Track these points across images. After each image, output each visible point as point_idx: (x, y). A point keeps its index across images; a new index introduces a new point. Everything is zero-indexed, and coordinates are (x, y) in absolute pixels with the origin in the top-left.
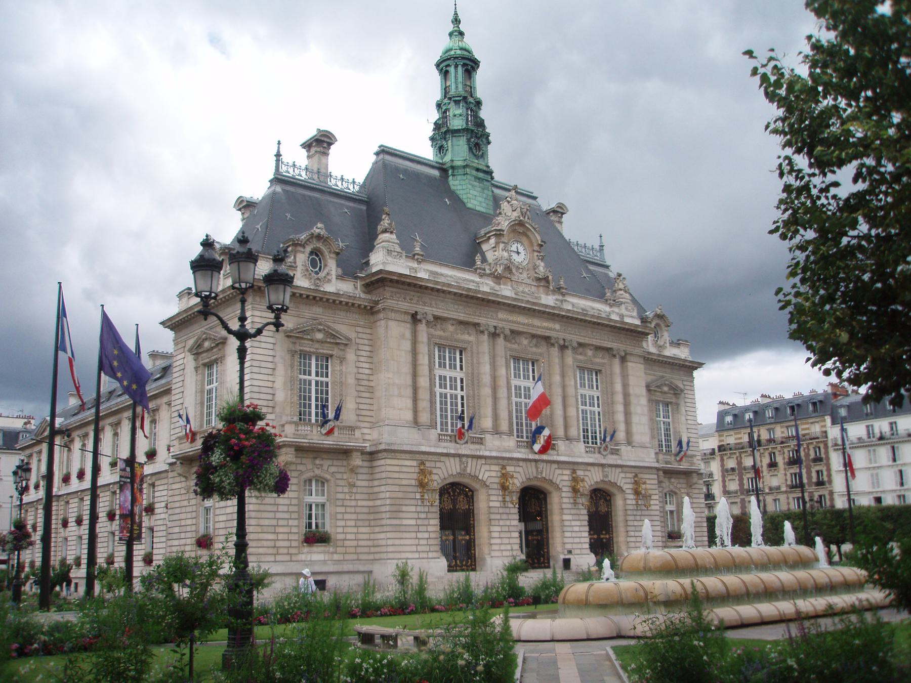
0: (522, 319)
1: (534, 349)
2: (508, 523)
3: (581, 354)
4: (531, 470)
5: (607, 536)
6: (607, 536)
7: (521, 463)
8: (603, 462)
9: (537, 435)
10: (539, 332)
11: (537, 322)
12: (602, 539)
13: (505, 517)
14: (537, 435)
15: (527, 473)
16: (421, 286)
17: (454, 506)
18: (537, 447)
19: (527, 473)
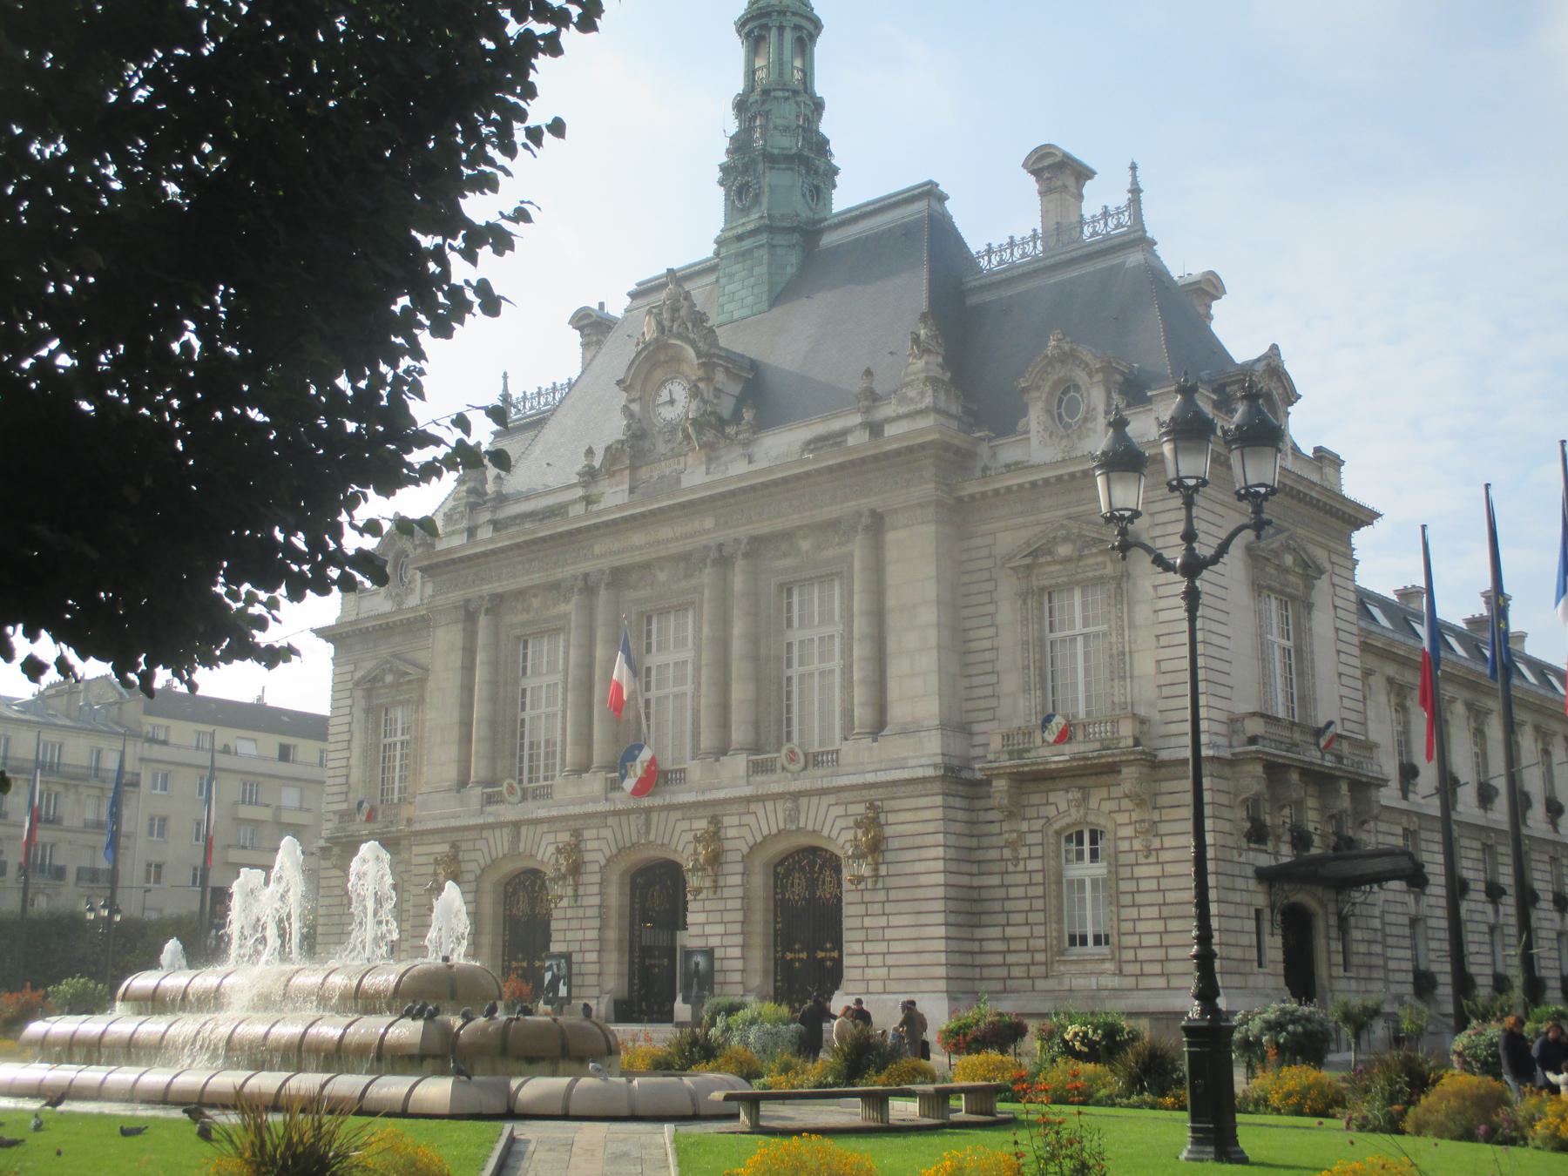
0: (638, 538)
1: (683, 584)
2: (580, 935)
3: (785, 555)
4: (631, 830)
5: (789, 956)
6: (789, 956)
7: (610, 821)
8: (796, 786)
9: (628, 764)
10: (674, 549)
11: (665, 532)
12: (823, 960)
13: (574, 924)
14: (628, 764)
15: (619, 836)
16: (461, 560)
17: (533, 909)
18: (629, 784)
19: (619, 836)
